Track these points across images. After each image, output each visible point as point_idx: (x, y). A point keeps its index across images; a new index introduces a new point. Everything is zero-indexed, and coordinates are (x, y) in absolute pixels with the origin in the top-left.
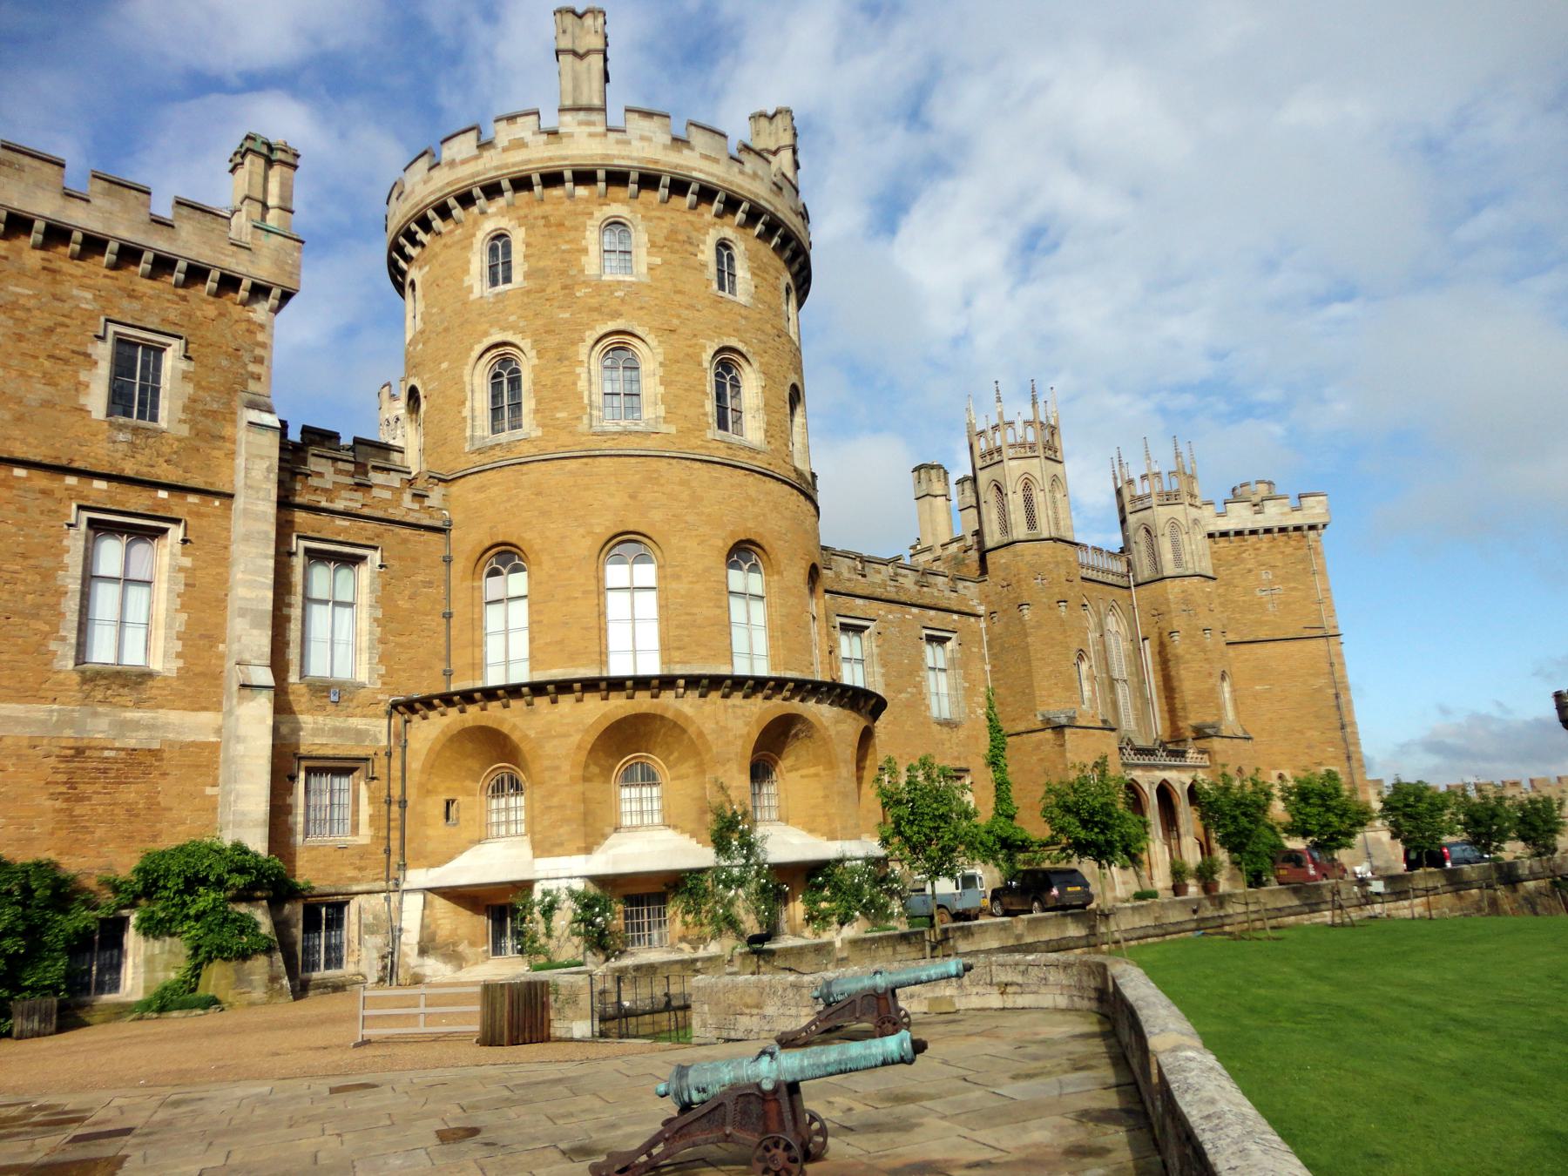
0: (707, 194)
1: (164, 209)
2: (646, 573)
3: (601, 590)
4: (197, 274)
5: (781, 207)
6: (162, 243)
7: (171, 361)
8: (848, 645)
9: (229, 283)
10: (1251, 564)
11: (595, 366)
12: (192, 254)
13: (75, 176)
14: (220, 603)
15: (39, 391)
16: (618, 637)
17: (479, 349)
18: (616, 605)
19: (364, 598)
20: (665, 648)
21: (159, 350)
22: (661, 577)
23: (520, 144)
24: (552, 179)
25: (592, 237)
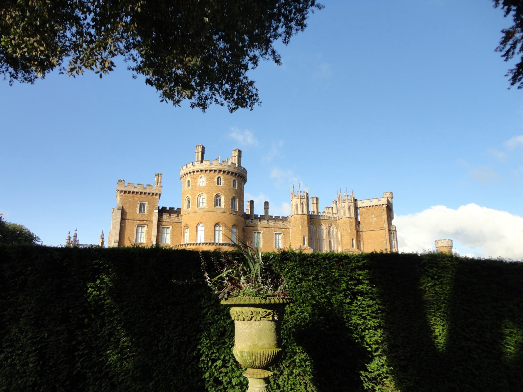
0: (215, 171)
1: (145, 186)
4: (149, 194)
6: (145, 191)
7: (146, 205)
9: (153, 194)
10: (370, 214)
13: (135, 185)
14: (151, 234)
15: (132, 211)
19: (170, 233)
21: (145, 204)
23: (190, 167)
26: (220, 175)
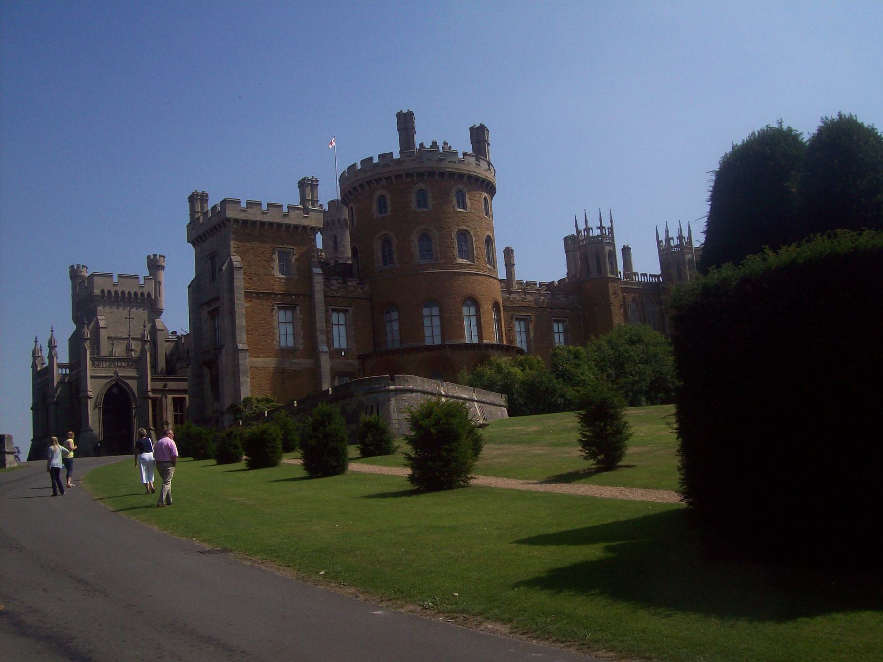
2: (435, 311)
3: (423, 317)
5: (481, 171)
6: (287, 221)
8: (518, 326)
11: (417, 242)
12: (294, 222)
16: (427, 332)
17: (378, 236)
18: (427, 322)
20: (443, 334)
22: (441, 311)
24: (398, 177)
25: (413, 198)
26: (460, 186)
